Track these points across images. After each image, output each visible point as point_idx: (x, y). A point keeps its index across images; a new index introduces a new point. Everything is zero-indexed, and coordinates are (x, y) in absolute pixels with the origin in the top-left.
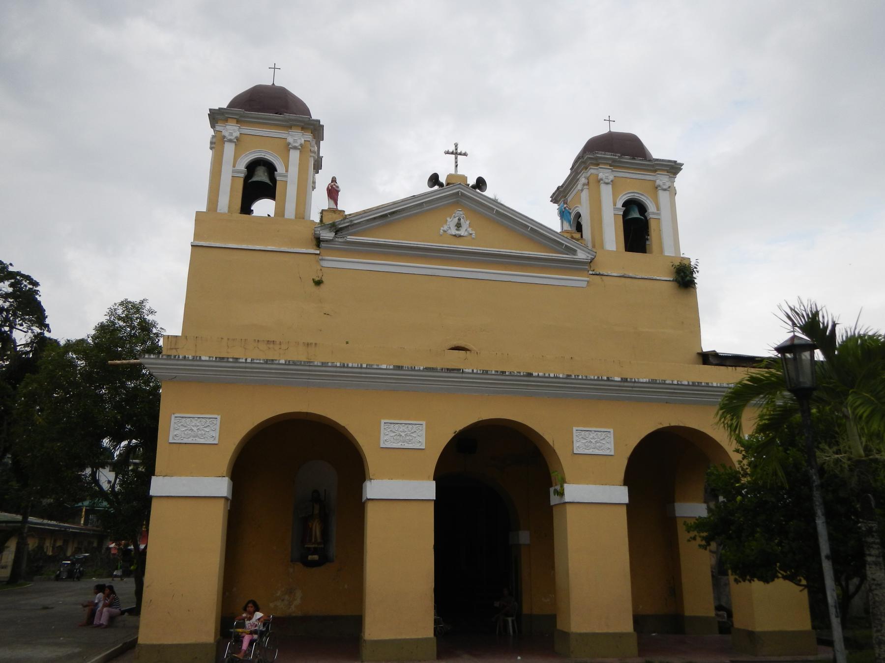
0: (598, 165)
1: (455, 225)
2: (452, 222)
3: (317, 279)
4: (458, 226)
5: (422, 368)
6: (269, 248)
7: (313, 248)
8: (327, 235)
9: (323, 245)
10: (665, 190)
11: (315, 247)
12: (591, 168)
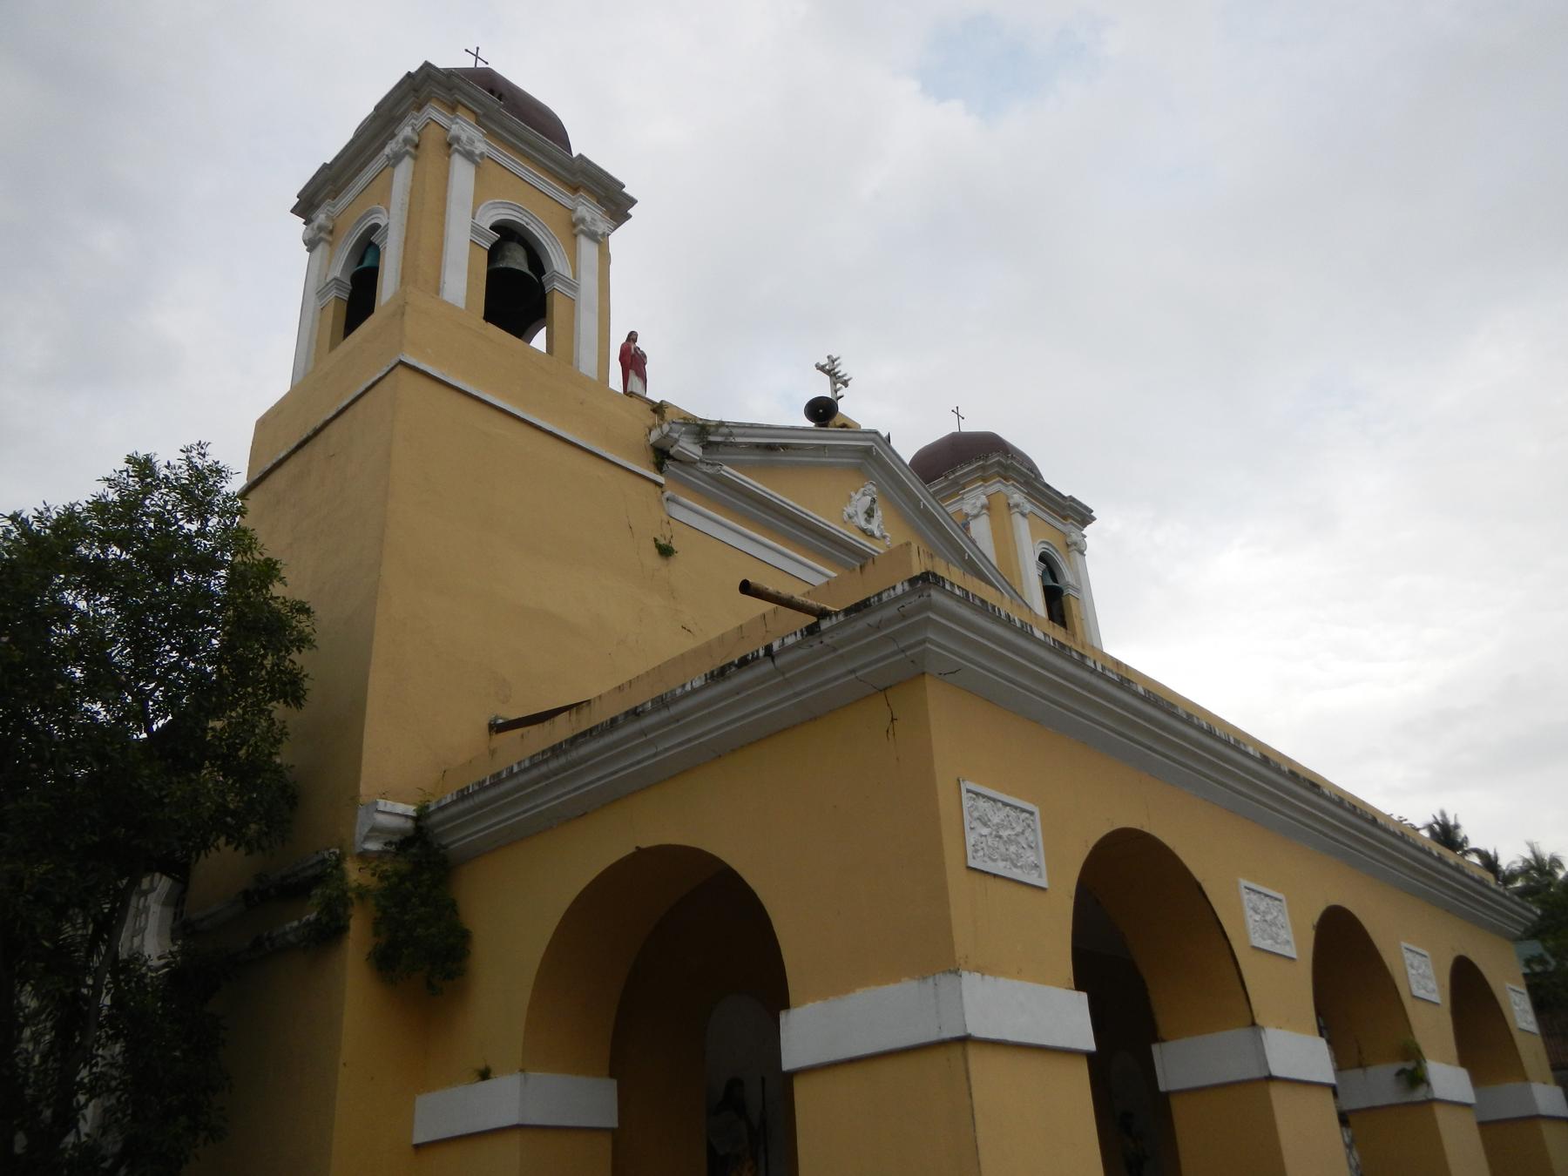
0: (1006, 479)
1: (864, 510)
3: (662, 542)
4: (870, 514)
7: (648, 468)
8: (690, 448)
9: (670, 466)
11: (652, 466)
12: (999, 482)
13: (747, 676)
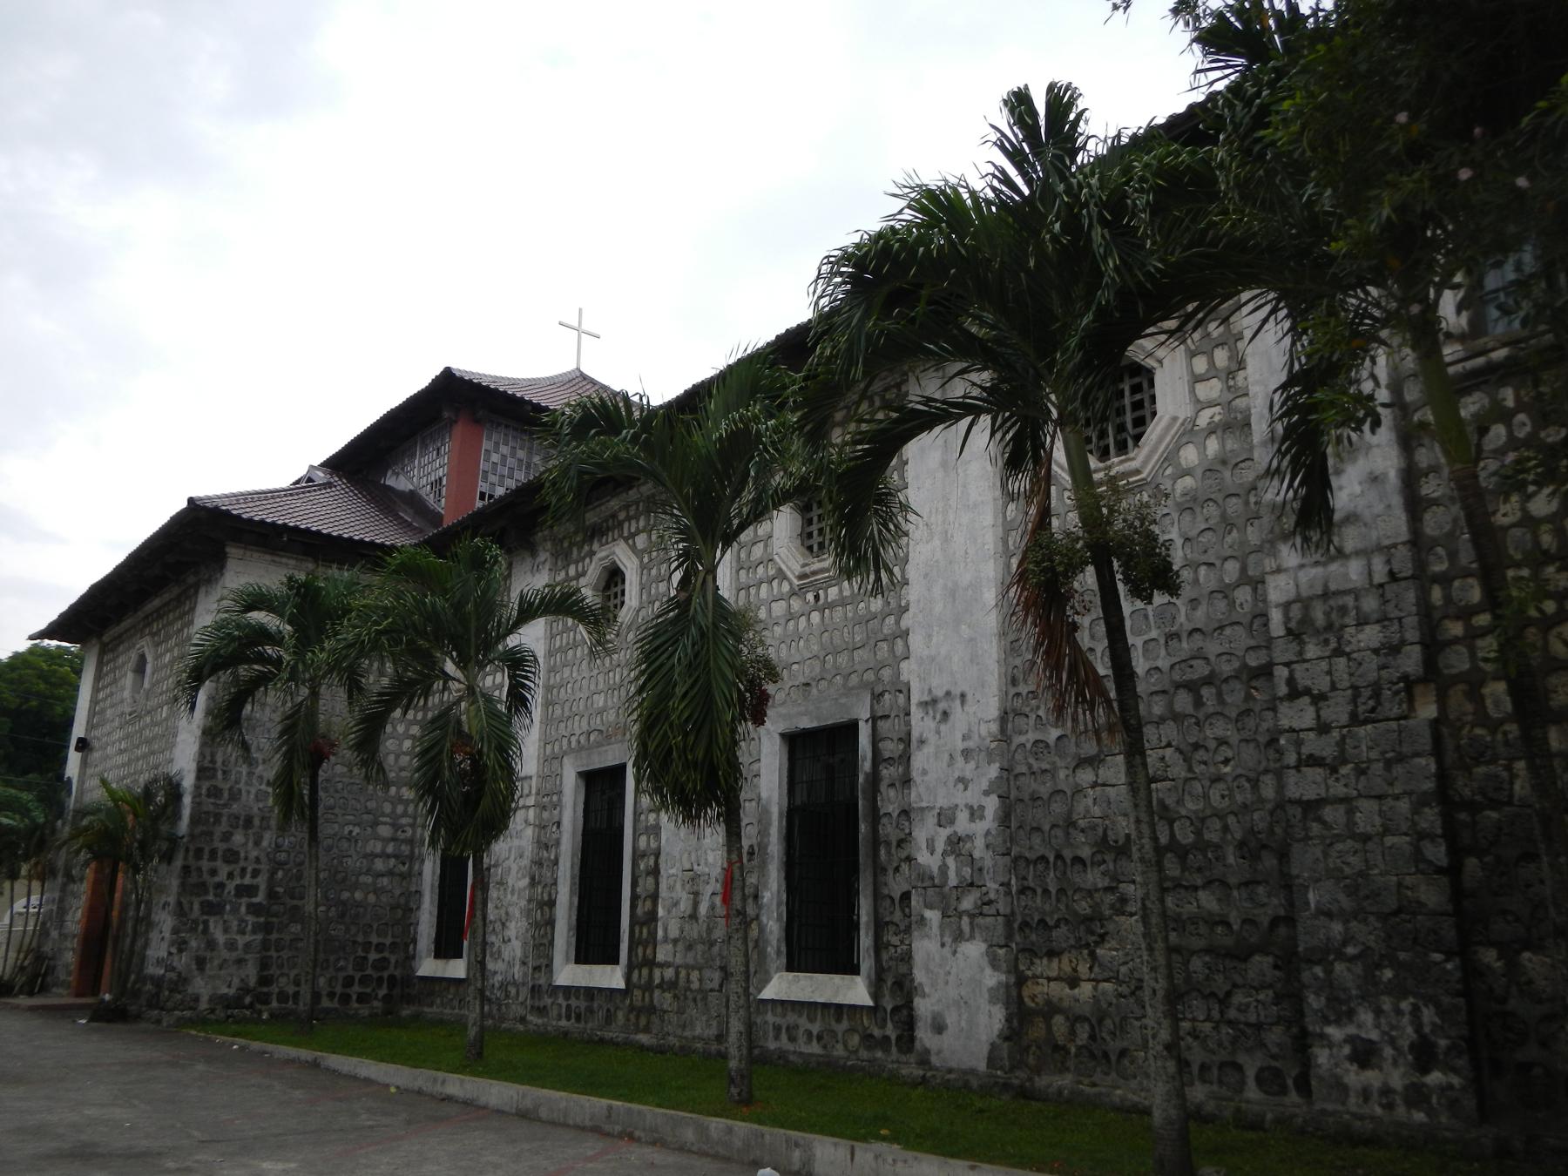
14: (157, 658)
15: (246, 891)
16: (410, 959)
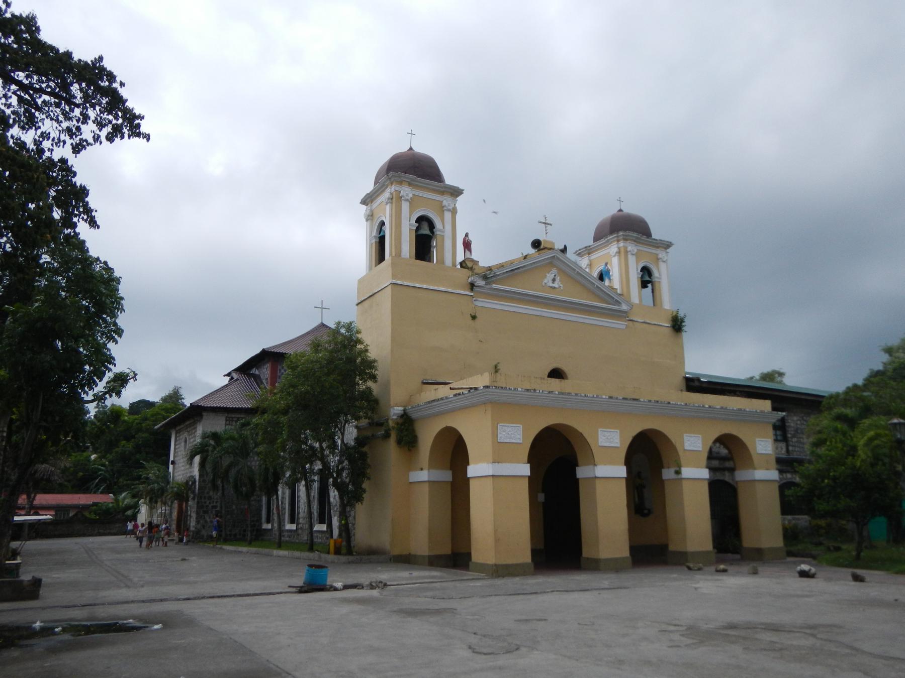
2: (550, 276)
3: (473, 314)
4: (554, 280)
5: (621, 398)
6: (441, 289)
8: (481, 283)
10: (664, 262)
11: (469, 290)
13: (460, 397)
14: (189, 439)
15: (215, 507)
16: (261, 524)
